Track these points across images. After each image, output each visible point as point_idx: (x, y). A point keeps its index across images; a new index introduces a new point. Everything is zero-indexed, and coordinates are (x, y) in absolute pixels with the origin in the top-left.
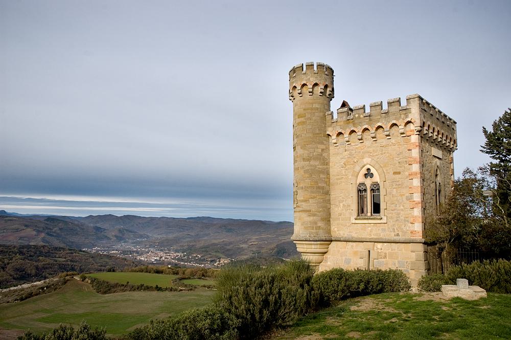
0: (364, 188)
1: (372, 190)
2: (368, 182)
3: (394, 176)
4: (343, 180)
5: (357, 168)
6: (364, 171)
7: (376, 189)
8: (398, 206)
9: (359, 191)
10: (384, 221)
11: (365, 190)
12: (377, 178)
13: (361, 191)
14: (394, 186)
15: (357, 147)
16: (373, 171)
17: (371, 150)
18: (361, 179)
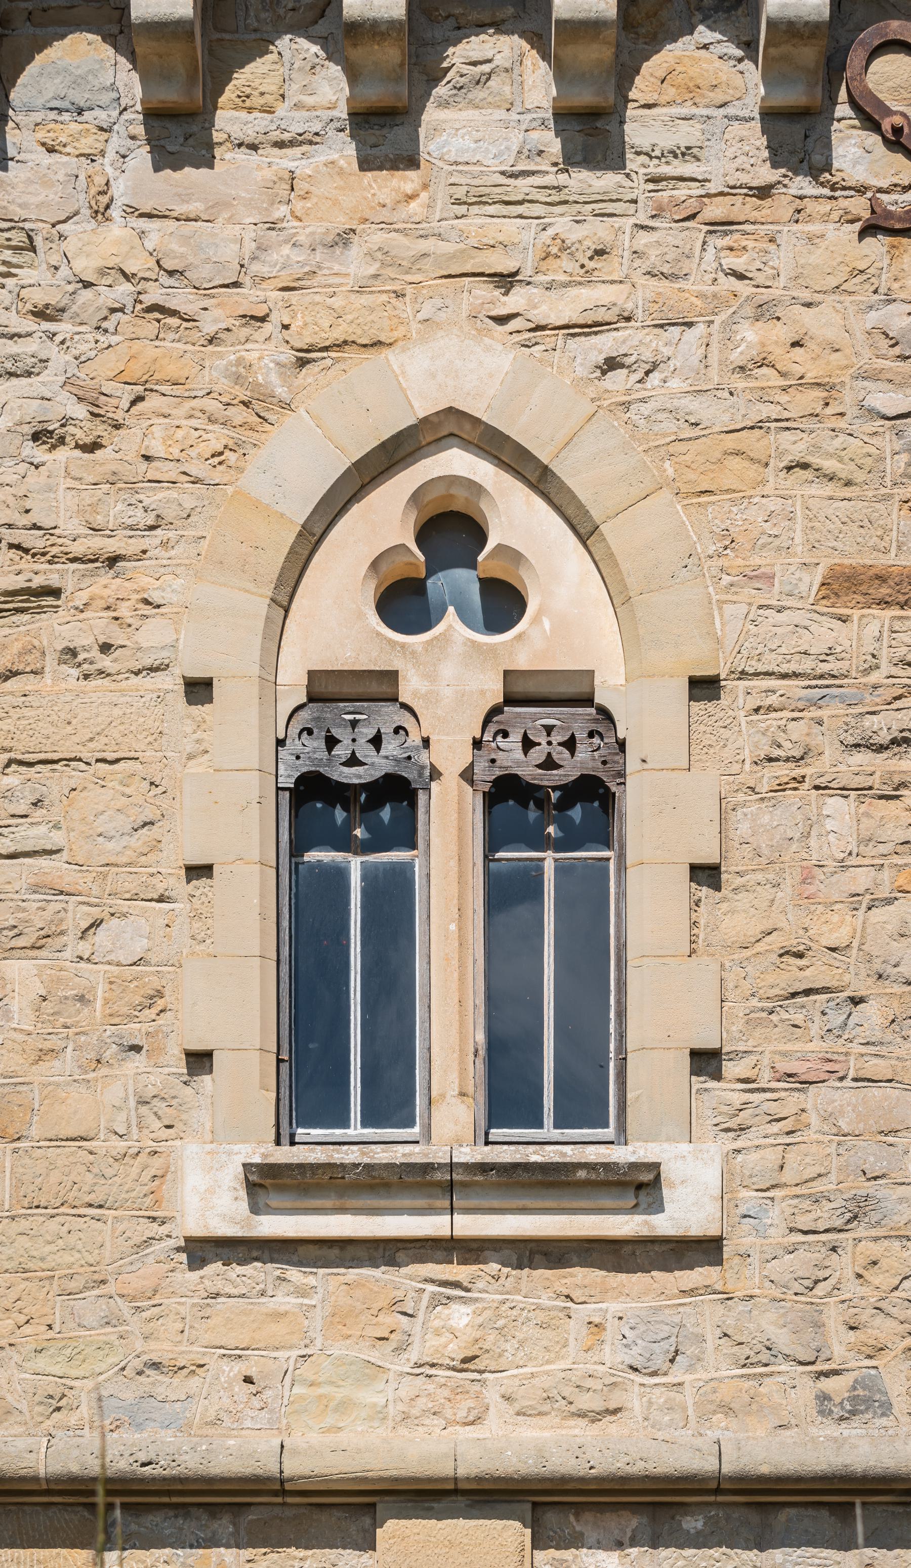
0: (376, 766)
1: (505, 795)
2: (449, 681)
3: (825, 633)
4: (54, 628)
5: (299, 460)
6: (385, 521)
7: (557, 802)
8: (872, 1016)
9: (312, 803)
10: (684, 1212)
11: (397, 795)
12: (571, 617)
13: (343, 806)
14: (831, 762)
15: (287, 160)
16: (515, 519)
17: (516, 239)
18: (338, 623)
